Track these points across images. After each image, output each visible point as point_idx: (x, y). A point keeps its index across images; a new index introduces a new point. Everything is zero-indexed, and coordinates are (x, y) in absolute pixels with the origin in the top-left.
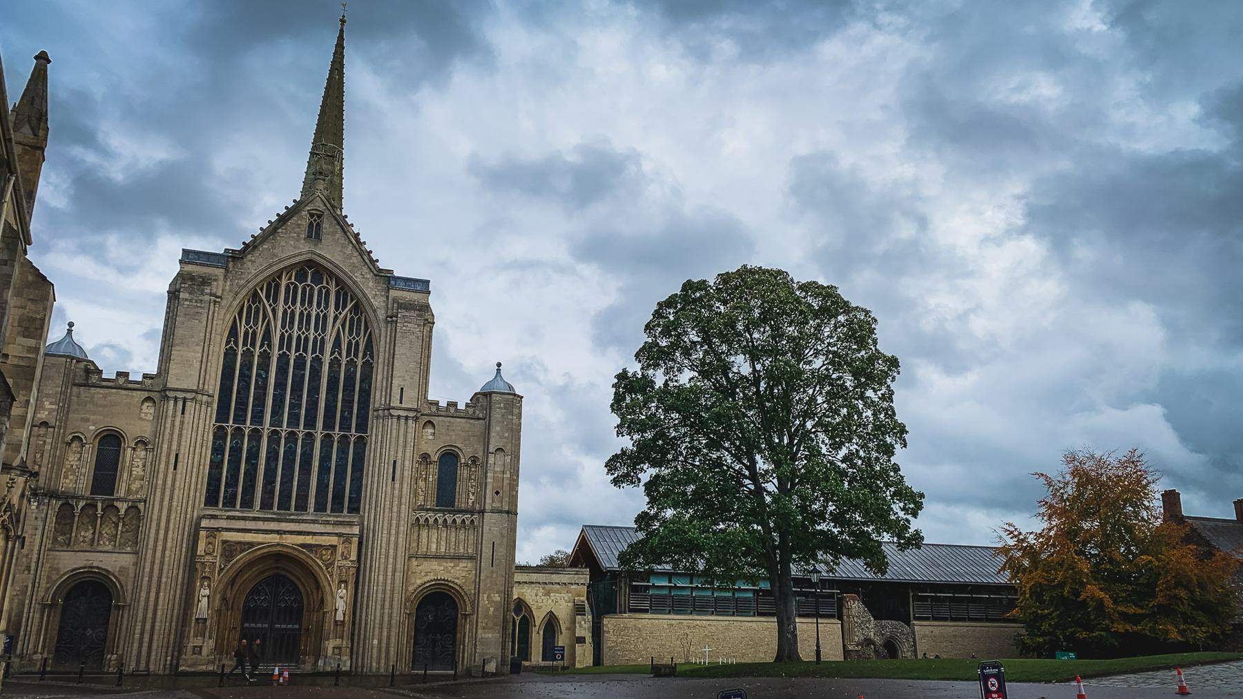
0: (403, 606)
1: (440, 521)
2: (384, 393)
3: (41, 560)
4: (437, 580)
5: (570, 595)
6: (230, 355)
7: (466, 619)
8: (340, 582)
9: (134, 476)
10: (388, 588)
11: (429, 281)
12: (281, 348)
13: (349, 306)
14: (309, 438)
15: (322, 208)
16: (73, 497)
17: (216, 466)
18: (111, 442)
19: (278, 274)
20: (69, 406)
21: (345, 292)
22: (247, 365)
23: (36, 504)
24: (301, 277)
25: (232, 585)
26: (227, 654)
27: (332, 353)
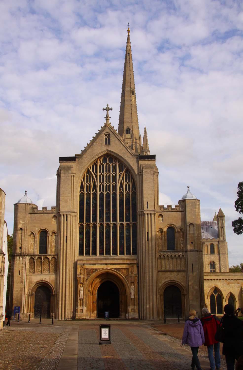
0: (157, 292)
1: (169, 256)
2: (141, 205)
3: (26, 279)
4: (170, 280)
5: (239, 284)
6: (82, 196)
7: (185, 296)
8: (131, 283)
9: (53, 246)
10: (151, 285)
11: (155, 155)
12: (100, 190)
13: (124, 170)
14: (115, 226)
15: (109, 131)
16: (33, 255)
17: (81, 240)
19: (96, 160)
20: (28, 222)
22: (88, 199)
23: (22, 258)
24: (105, 161)
25: (92, 285)
26: (93, 312)
27: (120, 190)
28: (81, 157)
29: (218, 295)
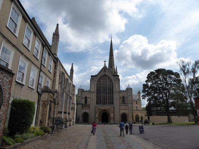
6: (97, 87)
17: (97, 100)
18: (86, 98)
21: (109, 78)
22: (99, 88)
24: (104, 77)
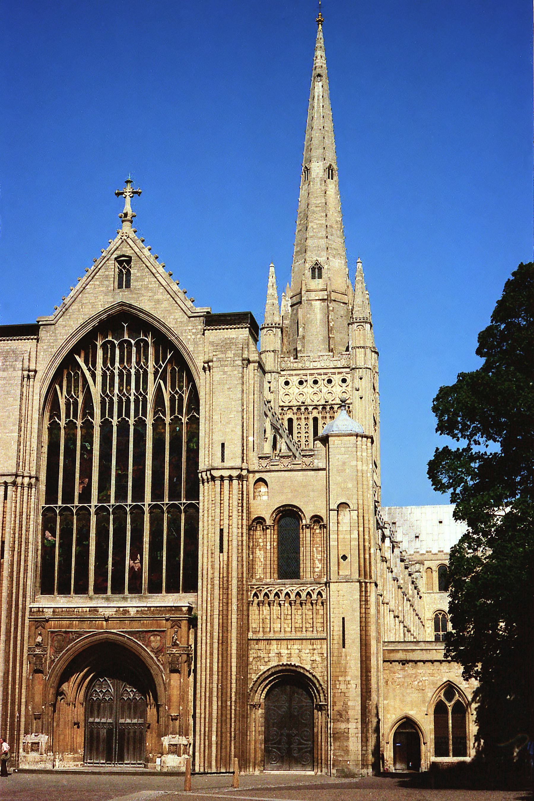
6: (54, 428)
15: (129, 252)
22: (71, 440)
27: (155, 413)
28: (54, 324)
29: (455, 704)
